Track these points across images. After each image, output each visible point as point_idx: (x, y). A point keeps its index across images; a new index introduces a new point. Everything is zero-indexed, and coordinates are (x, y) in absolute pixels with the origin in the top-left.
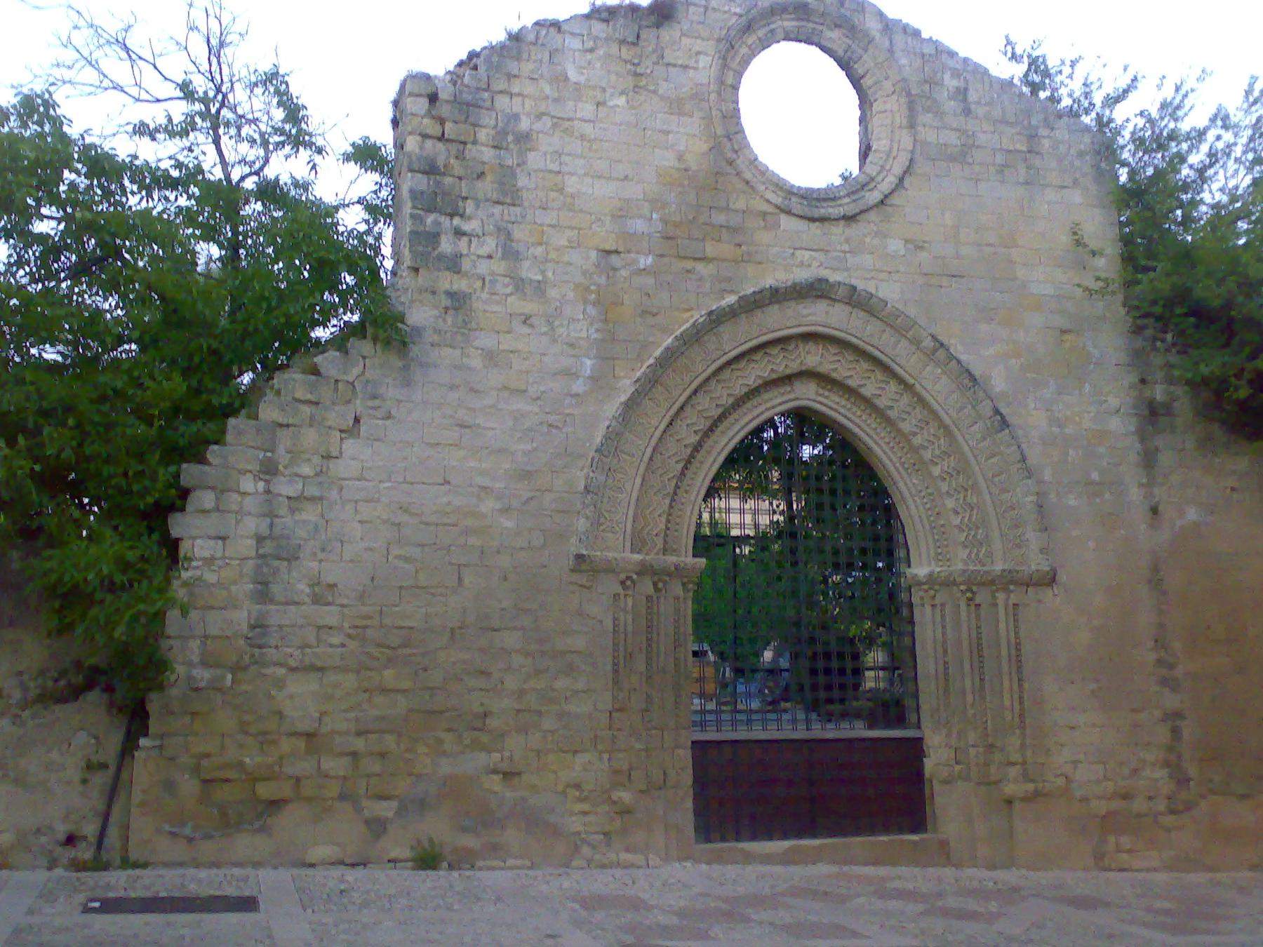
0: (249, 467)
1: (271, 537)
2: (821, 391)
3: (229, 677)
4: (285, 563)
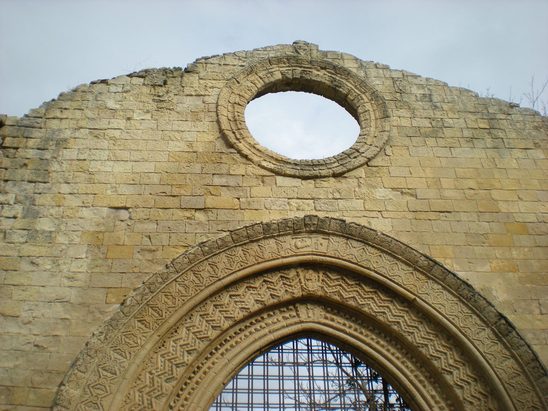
2: (328, 315)
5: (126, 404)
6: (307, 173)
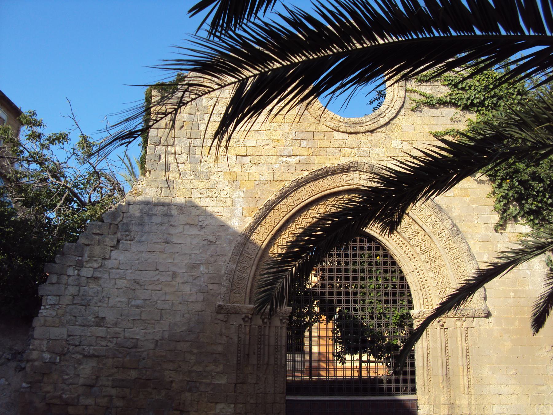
0: (71, 264)
1: (78, 295)
3: (58, 358)
4: (84, 307)
6: (352, 130)
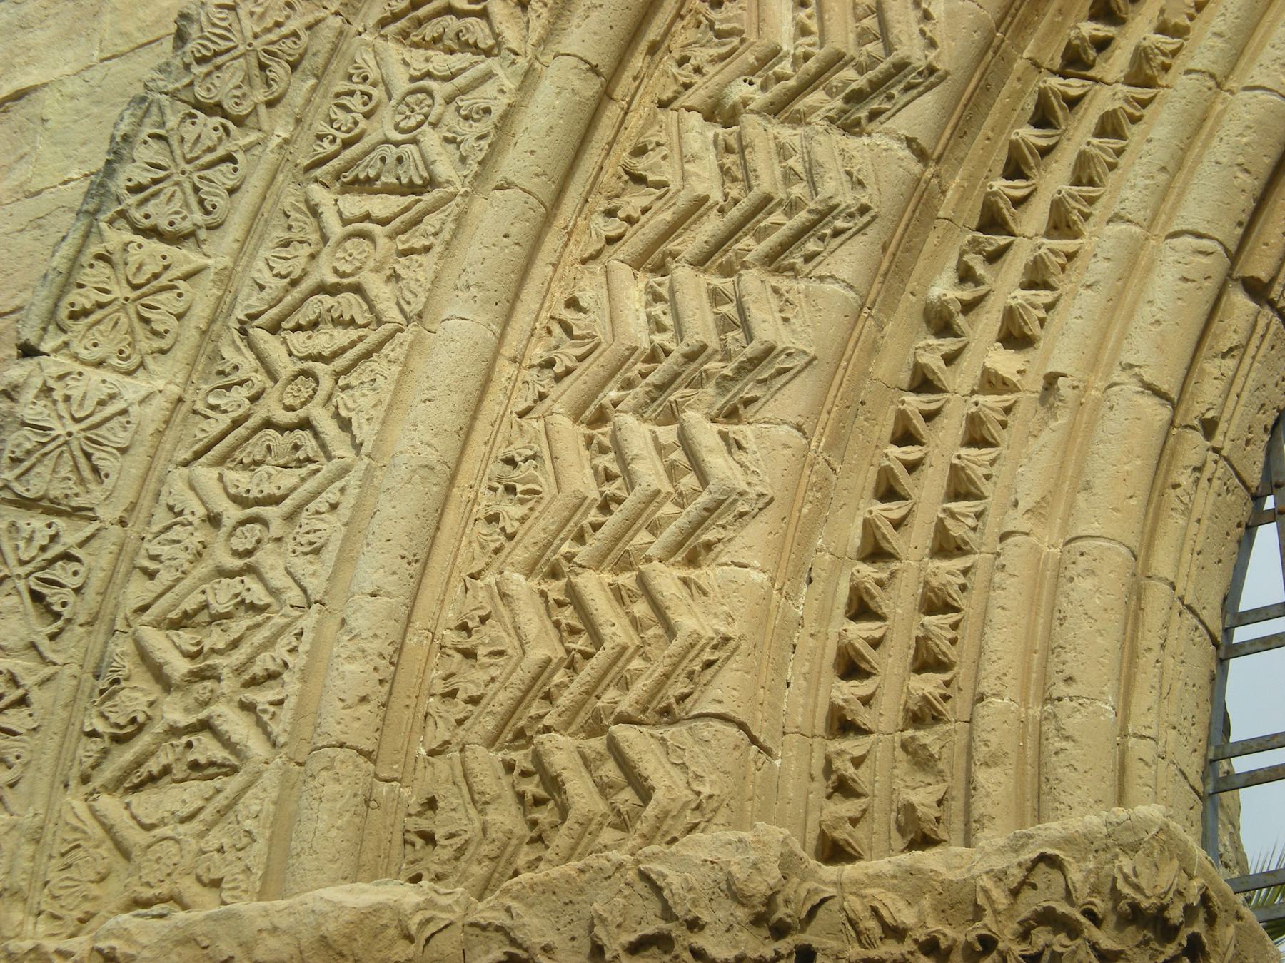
5: (558, 378)
